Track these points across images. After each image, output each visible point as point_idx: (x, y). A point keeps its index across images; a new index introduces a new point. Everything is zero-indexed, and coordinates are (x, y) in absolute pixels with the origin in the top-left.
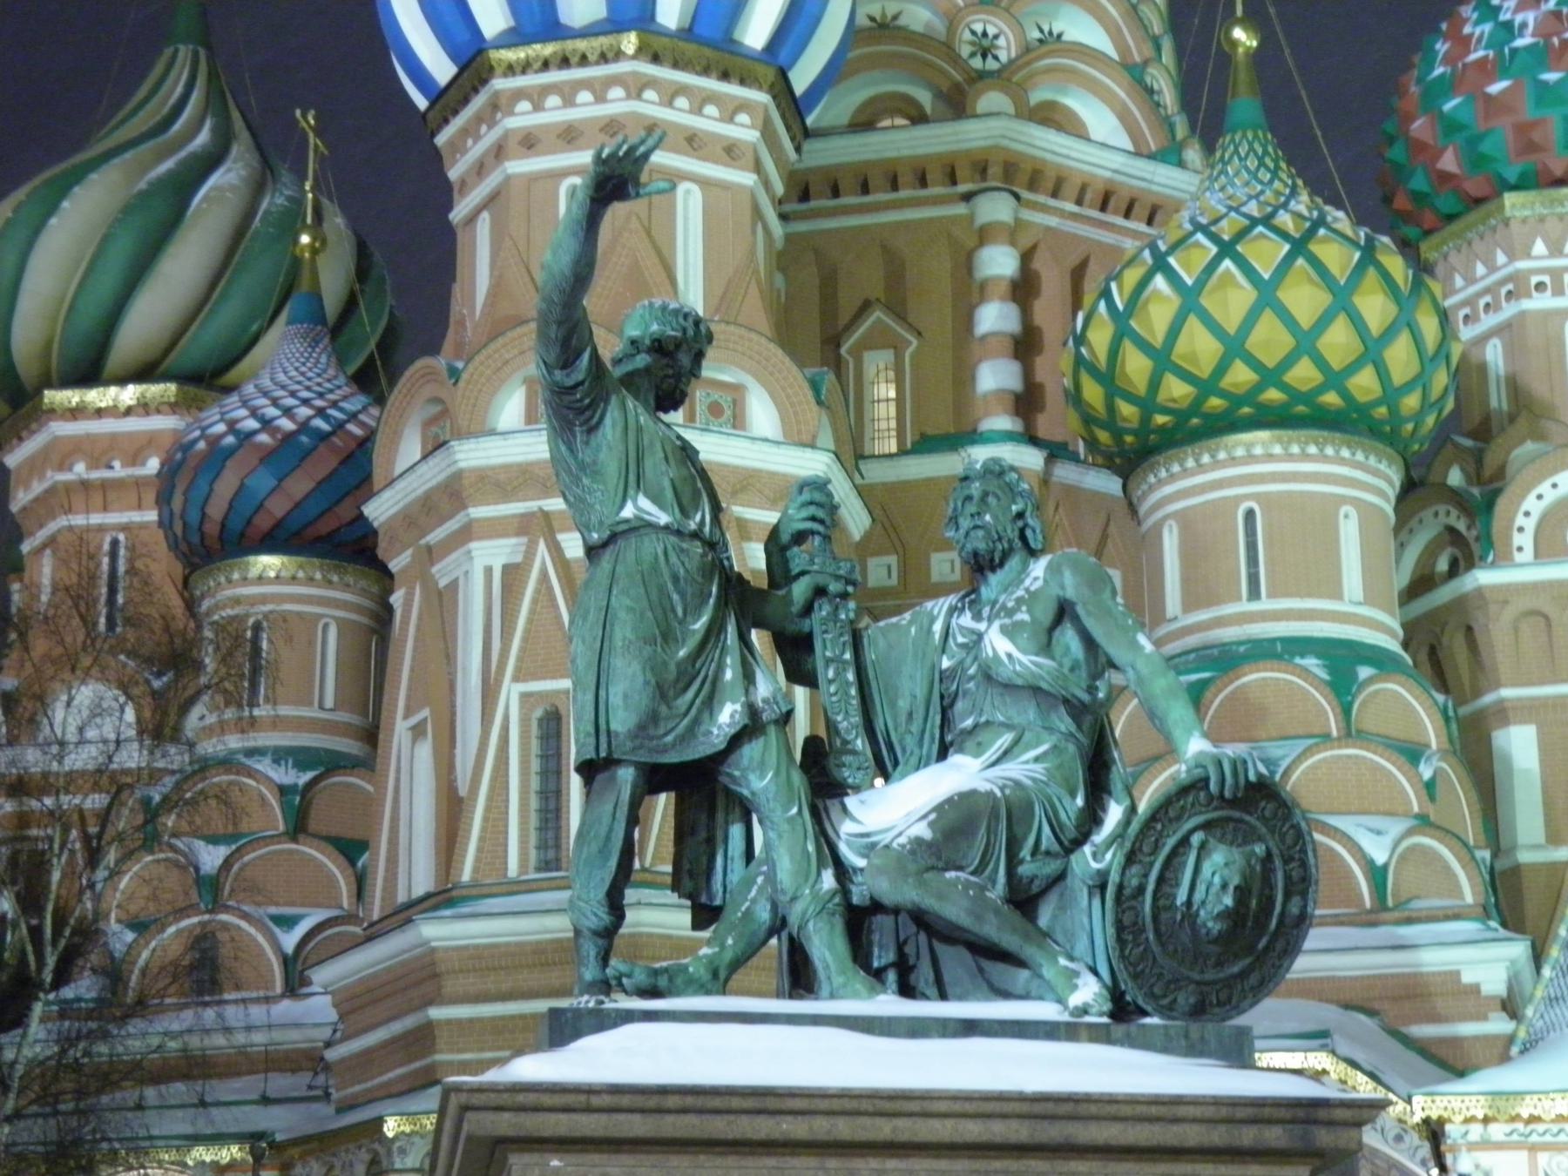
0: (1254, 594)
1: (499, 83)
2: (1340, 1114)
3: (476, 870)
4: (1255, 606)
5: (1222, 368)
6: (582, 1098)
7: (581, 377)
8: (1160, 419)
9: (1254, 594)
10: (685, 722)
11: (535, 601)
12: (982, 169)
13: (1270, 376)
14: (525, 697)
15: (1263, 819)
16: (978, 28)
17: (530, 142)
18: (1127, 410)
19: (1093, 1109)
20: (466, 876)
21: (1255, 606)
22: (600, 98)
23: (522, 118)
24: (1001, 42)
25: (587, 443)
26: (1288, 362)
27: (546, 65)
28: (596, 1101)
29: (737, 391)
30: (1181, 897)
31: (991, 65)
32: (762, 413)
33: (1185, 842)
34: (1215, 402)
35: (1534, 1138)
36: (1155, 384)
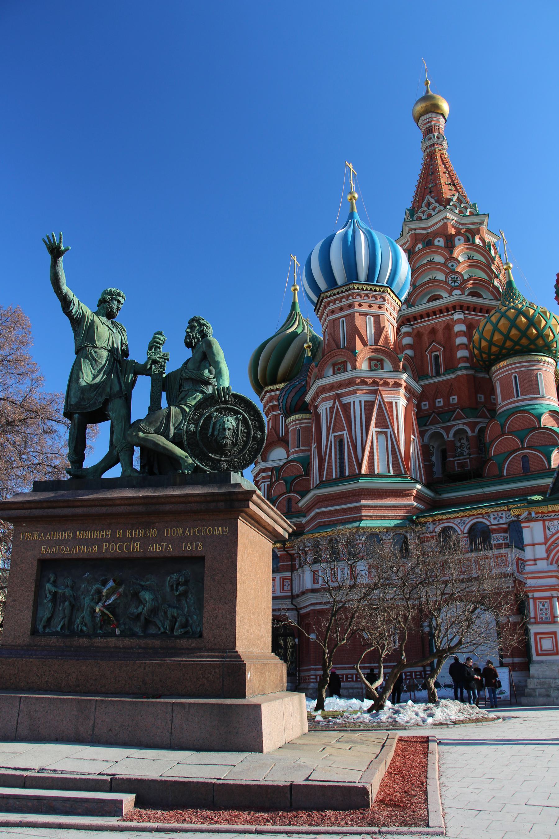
0: (518, 396)
1: (325, 300)
2: (240, 497)
3: (326, 477)
4: (518, 399)
5: (505, 343)
6: (21, 505)
7: (71, 309)
8: (492, 357)
9: (518, 396)
10: (94, 400)
11: (336, 414)
12: (454, 308)
13: (517, 343)
14: (334, 436)
15: (241, 407)
16: (453, 276)
17: (333, 312)
18: (484, 356)
19: (163, 500)
20: (324, 479)
21: (518, 399)
22: (347, 299)
23: (332, 307)
24: (458, 279)
25: (78, 328)
26: (520, 339)
27: (334, 295)
28: (25, 506)
29: (381, 361)
30: (210, 434)
31: (456, 284)
32: (388, 365)
33: (210, 417)
34: (504, 351)
35: (545, 518)
36: (490, 349)
